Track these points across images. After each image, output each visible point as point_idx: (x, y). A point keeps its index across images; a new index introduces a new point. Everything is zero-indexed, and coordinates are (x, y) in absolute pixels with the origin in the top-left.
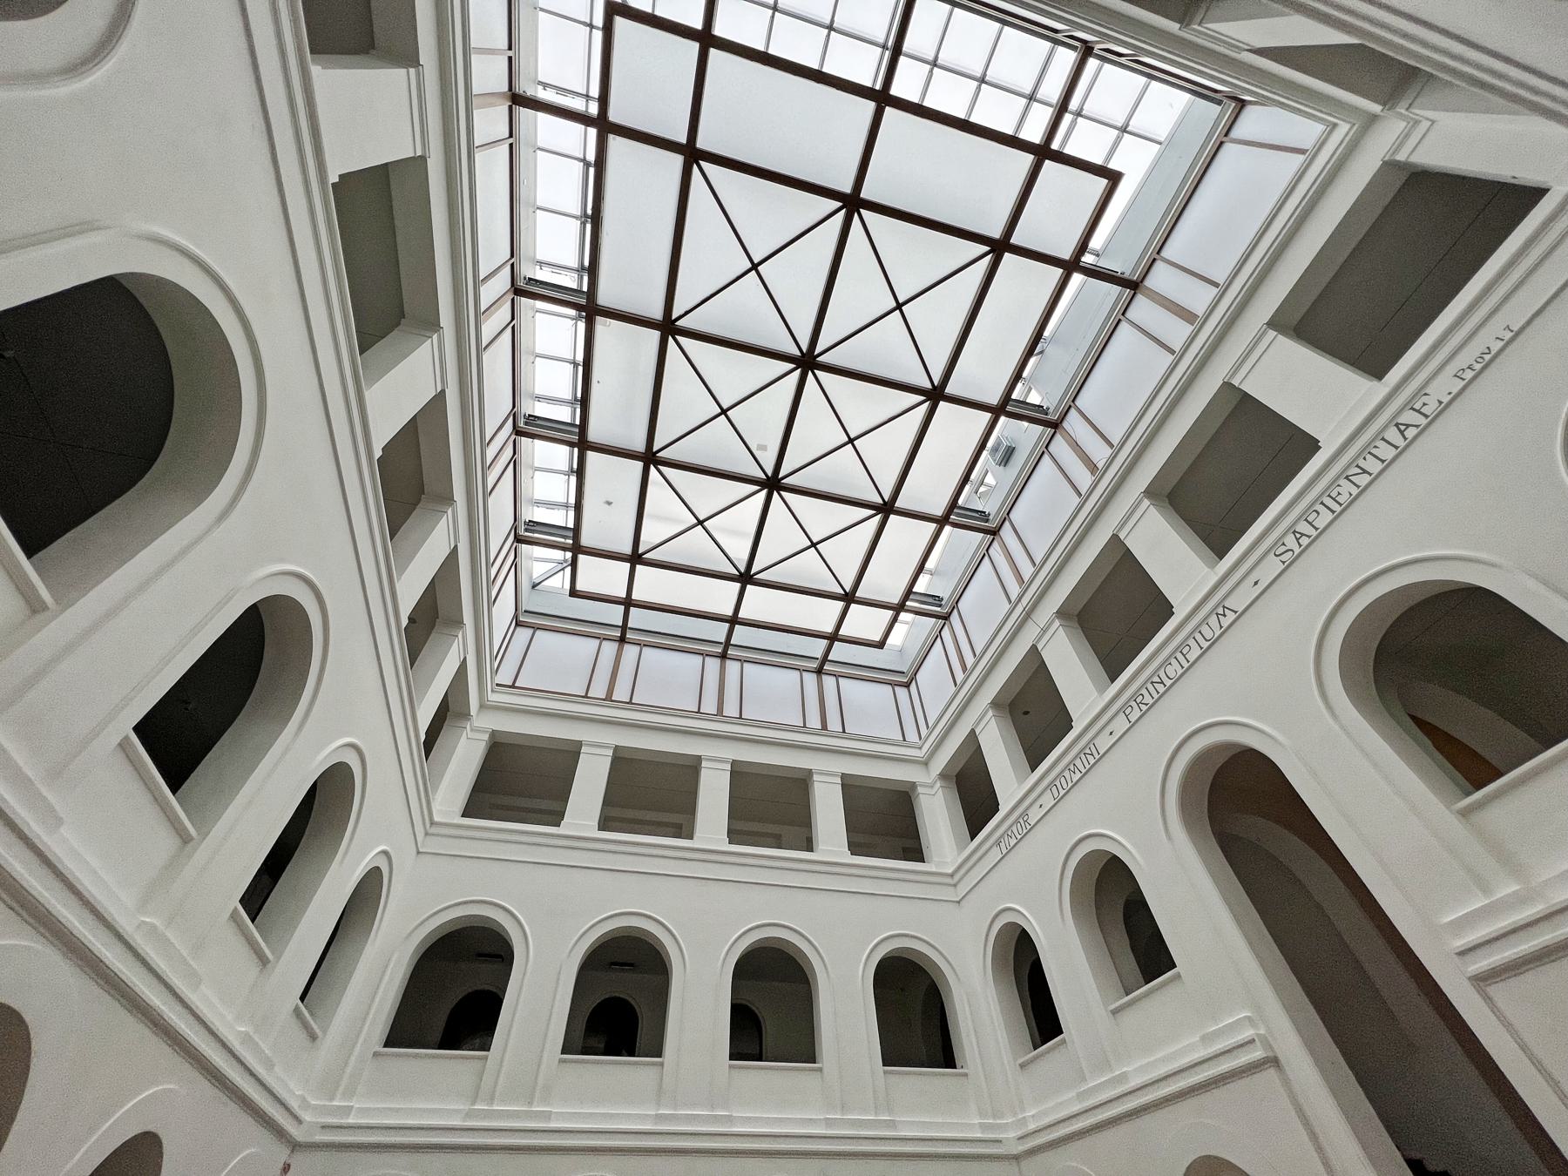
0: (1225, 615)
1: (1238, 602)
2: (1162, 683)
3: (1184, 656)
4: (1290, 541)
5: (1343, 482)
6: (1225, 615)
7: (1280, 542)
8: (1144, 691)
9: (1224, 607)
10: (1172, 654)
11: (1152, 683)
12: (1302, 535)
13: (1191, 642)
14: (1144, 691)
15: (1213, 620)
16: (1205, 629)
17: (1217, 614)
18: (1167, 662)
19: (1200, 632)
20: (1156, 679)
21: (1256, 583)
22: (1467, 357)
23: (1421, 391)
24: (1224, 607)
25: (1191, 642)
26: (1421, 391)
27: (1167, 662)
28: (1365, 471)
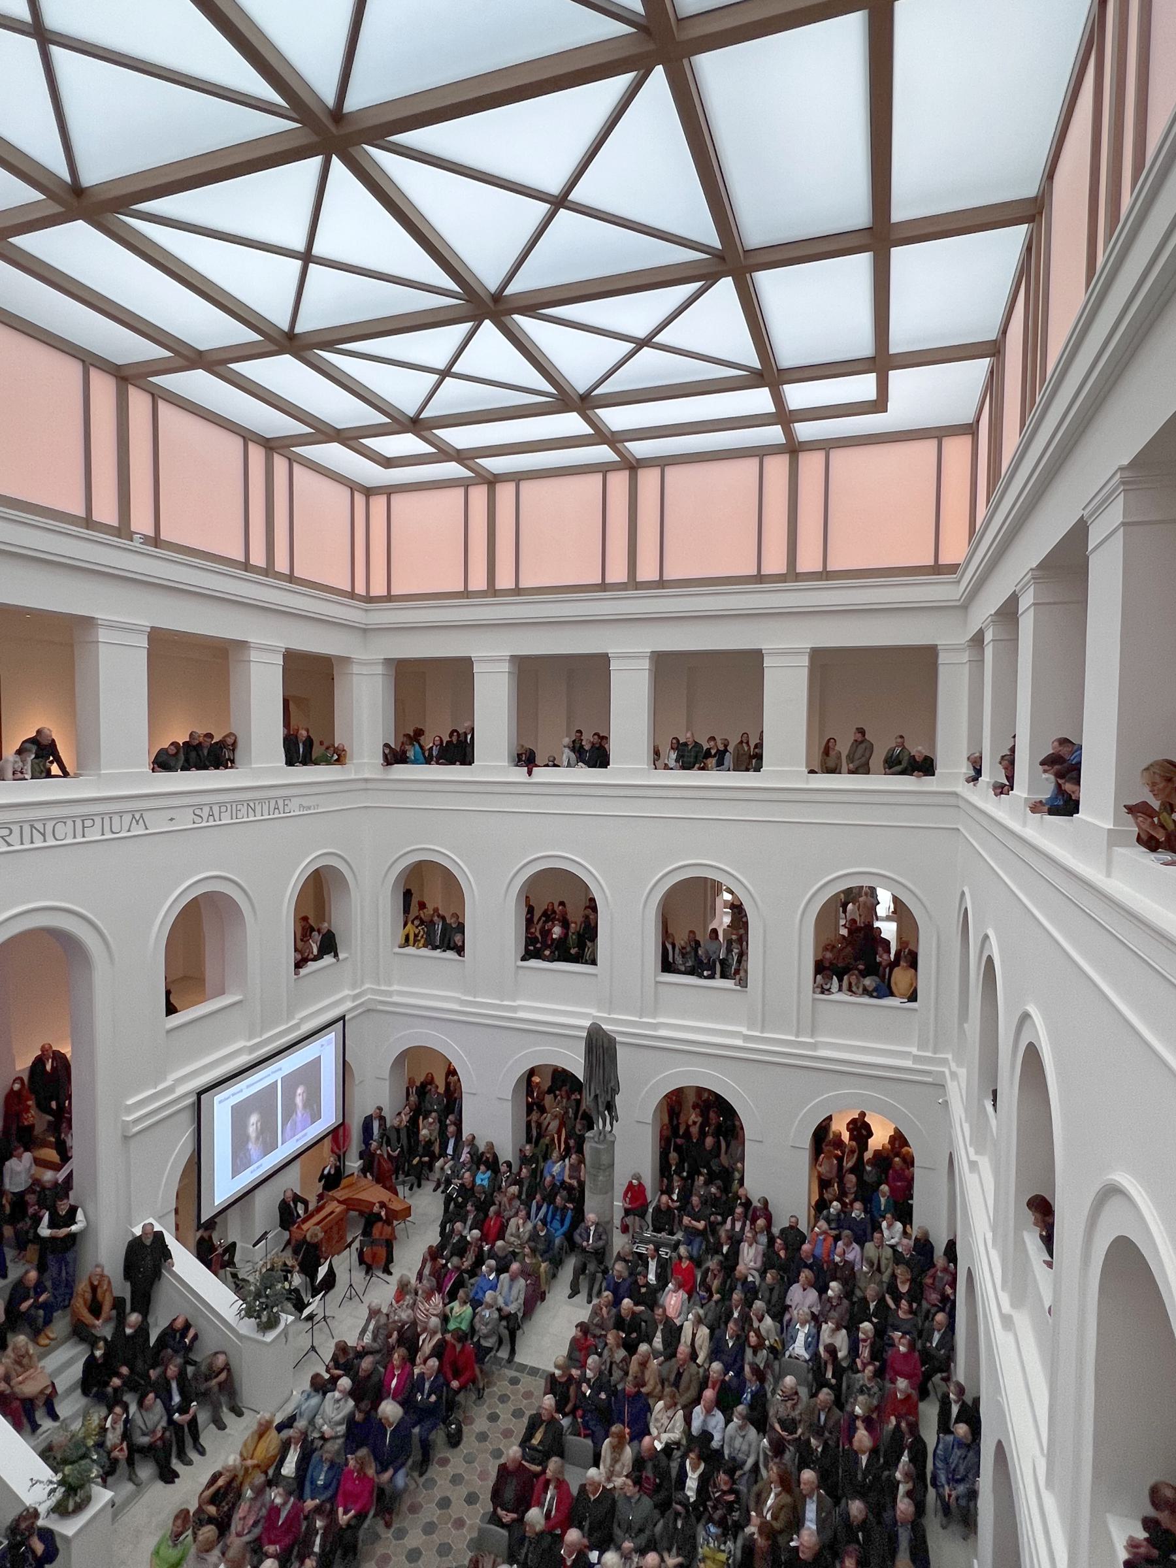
0: (137, 822)
1: (158, 824)
2: (44, 835)
3: (84, 827)
4: (206, 810)
5: (245, 805)
6: (137, 822)
7: (200, 807)
8: (16, 829)
9: (141, 816)
10: (73, 818)
11: (32, 826)
12: (213, 815)
13: (98, 820)
14: (16, 829)
15: (127, 818)
16: (116, 819)
17: (134, 817)
18: (62, 820)
19: (111, 818)
20: (39, 826)
21: (171, 819)
22: (305, 802)
23: (289, 798)
24: (141, 816)
25: (98, 820)
26: (289, 798)
27: (62, 820)
28: (254, 811)
